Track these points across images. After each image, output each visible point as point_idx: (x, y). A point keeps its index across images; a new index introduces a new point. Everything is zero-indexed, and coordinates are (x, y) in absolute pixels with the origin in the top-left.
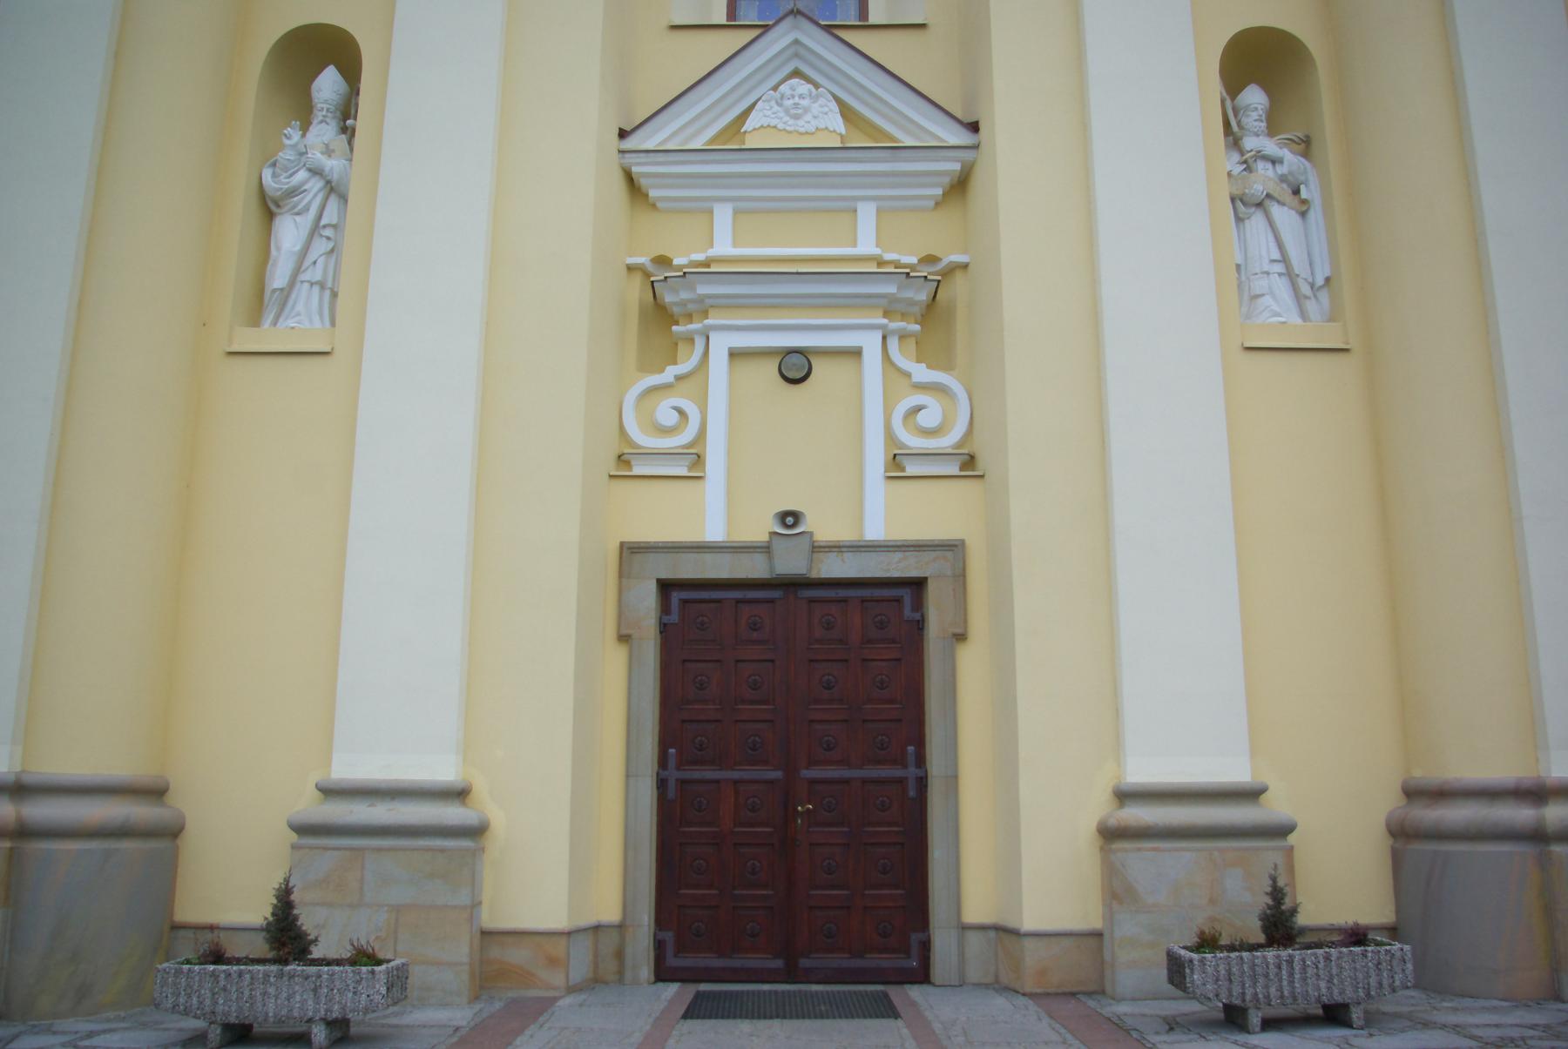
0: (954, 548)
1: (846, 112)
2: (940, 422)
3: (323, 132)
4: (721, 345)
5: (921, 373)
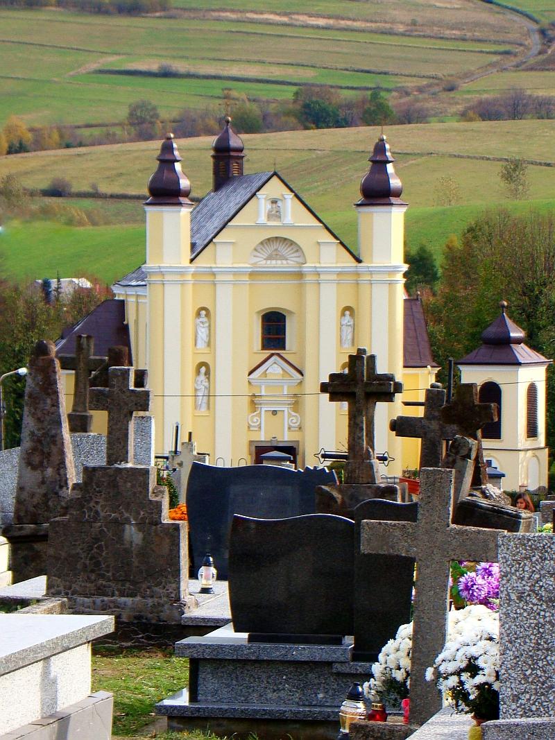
0: (298, 441)
1: (283, 369)
2: (295, 421)
3: (202, 377)
4: (263, 410)
5: (293, 414)
